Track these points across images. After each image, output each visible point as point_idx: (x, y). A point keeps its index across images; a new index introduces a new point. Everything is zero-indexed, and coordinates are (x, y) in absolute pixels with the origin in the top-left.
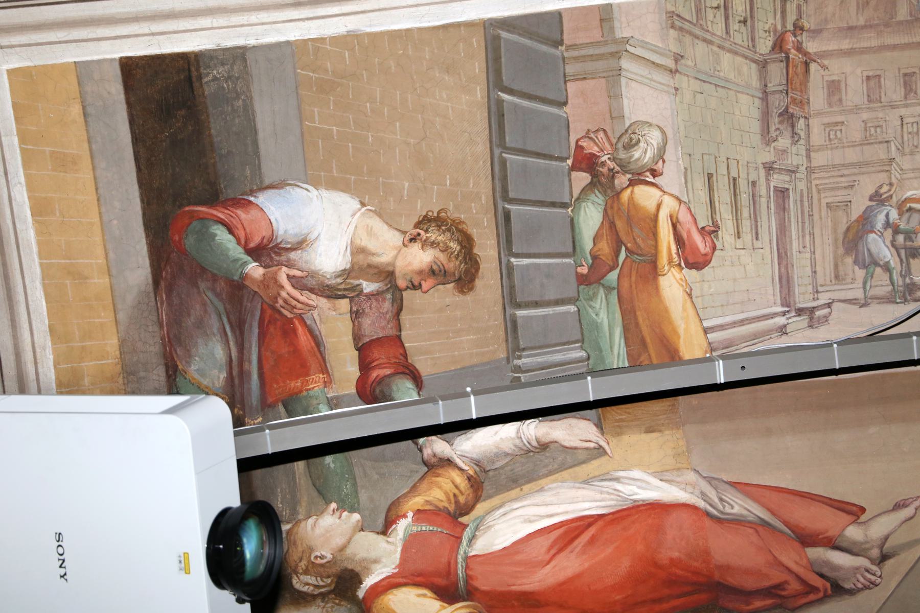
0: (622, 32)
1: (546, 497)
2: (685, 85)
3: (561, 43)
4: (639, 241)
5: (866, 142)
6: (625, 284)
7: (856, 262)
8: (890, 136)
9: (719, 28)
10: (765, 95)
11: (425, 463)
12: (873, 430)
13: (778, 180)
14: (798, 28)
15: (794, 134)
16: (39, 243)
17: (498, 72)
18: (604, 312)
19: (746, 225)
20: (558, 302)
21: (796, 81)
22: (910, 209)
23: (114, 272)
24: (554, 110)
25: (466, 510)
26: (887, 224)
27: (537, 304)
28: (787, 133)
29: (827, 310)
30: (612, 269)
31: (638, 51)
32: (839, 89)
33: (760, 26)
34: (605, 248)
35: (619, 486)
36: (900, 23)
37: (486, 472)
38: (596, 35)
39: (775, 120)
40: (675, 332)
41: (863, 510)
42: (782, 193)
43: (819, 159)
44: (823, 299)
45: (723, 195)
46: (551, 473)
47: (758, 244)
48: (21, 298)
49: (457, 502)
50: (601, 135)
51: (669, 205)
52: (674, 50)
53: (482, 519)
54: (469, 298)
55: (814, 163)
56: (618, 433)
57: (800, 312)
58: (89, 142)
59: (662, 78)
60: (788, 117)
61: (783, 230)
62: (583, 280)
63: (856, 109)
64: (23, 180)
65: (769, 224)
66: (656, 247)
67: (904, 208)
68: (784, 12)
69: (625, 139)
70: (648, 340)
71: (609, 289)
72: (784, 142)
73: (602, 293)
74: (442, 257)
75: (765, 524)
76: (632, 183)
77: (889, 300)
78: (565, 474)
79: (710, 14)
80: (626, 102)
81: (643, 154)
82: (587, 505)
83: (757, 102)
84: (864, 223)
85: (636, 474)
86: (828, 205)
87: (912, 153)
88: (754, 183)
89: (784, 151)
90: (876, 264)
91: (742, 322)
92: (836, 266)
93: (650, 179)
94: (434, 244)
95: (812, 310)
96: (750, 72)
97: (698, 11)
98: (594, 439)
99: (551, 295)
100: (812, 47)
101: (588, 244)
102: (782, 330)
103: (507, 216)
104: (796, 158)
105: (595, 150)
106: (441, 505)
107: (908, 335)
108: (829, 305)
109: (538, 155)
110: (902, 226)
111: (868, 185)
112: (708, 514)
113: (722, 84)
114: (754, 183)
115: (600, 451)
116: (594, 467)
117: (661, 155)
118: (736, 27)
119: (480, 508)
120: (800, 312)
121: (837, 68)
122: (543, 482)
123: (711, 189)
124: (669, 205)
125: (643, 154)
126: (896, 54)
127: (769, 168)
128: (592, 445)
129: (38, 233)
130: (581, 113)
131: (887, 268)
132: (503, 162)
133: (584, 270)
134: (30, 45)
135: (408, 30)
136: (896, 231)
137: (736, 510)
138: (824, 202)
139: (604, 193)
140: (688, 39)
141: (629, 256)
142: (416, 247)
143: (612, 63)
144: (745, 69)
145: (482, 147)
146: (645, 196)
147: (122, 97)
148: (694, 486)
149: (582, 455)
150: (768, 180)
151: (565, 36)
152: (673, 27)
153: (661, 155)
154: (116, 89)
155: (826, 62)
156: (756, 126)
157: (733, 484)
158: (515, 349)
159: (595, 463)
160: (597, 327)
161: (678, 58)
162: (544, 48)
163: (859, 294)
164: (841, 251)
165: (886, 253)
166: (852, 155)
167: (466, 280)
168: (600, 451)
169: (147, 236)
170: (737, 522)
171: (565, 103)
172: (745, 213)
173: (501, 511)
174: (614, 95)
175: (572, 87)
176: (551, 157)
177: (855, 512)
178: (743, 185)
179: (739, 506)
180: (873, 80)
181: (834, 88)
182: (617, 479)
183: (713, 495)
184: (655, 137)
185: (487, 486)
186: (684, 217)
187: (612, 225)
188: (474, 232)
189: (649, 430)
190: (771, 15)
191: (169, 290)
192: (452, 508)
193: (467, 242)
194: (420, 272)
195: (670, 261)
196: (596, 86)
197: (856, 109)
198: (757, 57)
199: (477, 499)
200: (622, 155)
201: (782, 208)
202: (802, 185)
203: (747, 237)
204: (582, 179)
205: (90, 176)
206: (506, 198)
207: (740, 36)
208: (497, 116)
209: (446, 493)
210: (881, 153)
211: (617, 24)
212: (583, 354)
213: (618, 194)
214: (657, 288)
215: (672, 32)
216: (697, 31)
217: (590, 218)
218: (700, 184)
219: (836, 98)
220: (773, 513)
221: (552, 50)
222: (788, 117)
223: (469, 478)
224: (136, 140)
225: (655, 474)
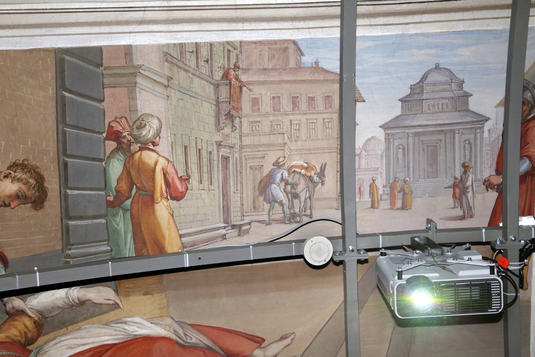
0: (137, 61)
1: (83, 333)
2: (173, 95)
3: (102, 65)
4: (144, 183)
5: (272, 133)
6: (135, 207)
7: (265, 200)
8: (285, 131)
9: (193, 64)
10: (218, 103)
11: (7, 313)
12: (271, 295)
13: (224, 151)
14: (236, 67)
15: (233, 126)
17: (63, 79)
18: (122, 224)
19: (205, 176)
20: (95, 217)
21: (235, 97)
22: (294, 171)
24: (97, 104)
25: (32, 341)
26: (282, 179)
27: (81, 218)
28: (230, 126)
29: (247, 227)
30: (128, 198)
31: (147, 73)
32: (258, 103)
33: (216, 64)
34: (124, 186)
35: (126, 327)
36: (291, 69)
37: (46, 318)
38: (122, 62)
39: (223, 118)
40: (163, 236)
41: (264, 340)
42: (226, 159)
43: (247, 141)
44: (247, 220)
45: (193, 158)
46: (85, 319)
47: (212, 187)
49: (26, 337)
50: (124, 120)
51: (162, 163)
52: (167, 74)
53: (41, 347)
54: (40, 213)
55: (244, 144)
56: (127, 294)
57: (234, 227)
59: (160, 89)
60: (230, 116)
61: (226, 180)
62: (110, 204)
63: (267, 115)
65: (218, 176)
66: (154, 186)
67: (291, 171)
68: (229, 58)
69: (138, 123)
70: (147, 240)
71: (125, 210)
72: (227, 130)
73: (121, 212)
74: (24, 188)
75: (209, 348)
76: (141, 149)
77: (282, 221)
78: (94, 319)
79: (188, 55)
80: (138, 102)
81: (148, 133)
82: (106, 338)
83: (213, 107)
84: (270, 179)
85: (137, 319)
86: (251, 167)
87: (296, 141)
88: (210, 153)
89: (228, 136)
90: (275, 201)
91: (201, 232)
92: (254, 201)
93: (151, 147)
94: (19, 180)
95: (240, 226)
96: (210, 90)
97: (181, 53)
98: (113, 298)
99: (91, 213)
100: (244, 78)
101: (114, 184)
102: (224, 237)
103: (66, 164)
104: (234, 140)
105: (120, 128)
106: (16, 339)
107: (290, 242)
108: (249, 224)
109: (86, 130)
110: (290, 181)
111: (272, 157)
112: (177, 343)
113: (194, 96)
114: (210, 153)
115: (116, 306)
116: (112, 315)
117: (158, 134)
118: (203, 64)
119: (41, 340)
120: (234, 227)
121: (257, 91)
122: (80, 324)
123: (186, 155)
124: (162, 163)
125: (148, 133)
126: (288, 85)
127: (219, 145)
128: (111, 302)
130: (112, 106)
131: (281, 204)
132: (64, 133)
133: (111, 199)
135: (7, 51)
136: (287, 183)
137: (194, 340)
138: (248, 165)
139: (125, 154)
140: (175, 69)
141: (138, 192)
142: (8, 181)
143: (132, 79)
144: (207, 88)
145: (51, 123)
146: (149, 157)
148: (170, 326)
149: (105, 308)
150: (218, 151)
151: (104, 61)
152: (167, 61)
153: (158, 134)
155: (251, 87)
156: (212, 121)
157: (193, 326)
158: (67, 244)
159: (112, 313)
160: (117, 232)
161: (169, 79)
162: (91, 67)
163: (266, 218)
164: (257, 193)
165: (281, 195)
166: (264, 140)
167: (38, 200)
168: (116, 306)
170: (194, 347)
171: (103, 101)
172: (205, 169)
173: (54, 342)
174: (132, 97)
175: (107, 91)
176: (93, 132)
177: (259, 341)
178: (204, 154)
179: (196, 338)
180: (276, 99)
181: (255, 102)
182: (125, 323)
183: (181, 332)
184: (155, 123)
185: (46, 327)
186: (170, 170)
187: (129, 173)
188: (45, 173)
189: (145, 294)
190: (222, 59)
192: (23, 340)
193: (40, 180)
194: (10, 196)
195: (162, 195)
196: (121, 92)
197: (267, 115)
198: (213, 82)
199: (39, 335)
200: (136, 132)
201: (226, 168)
202: (237, 155)
203: (206, 183)
204: (111, 145)
206: (65, 154)
207: (204, 69)
208: (62, 106)
209: (20, 331)
210: (279, 139)
211: (134, 57)
212: (109, 248)
213: (133, 155)
214: (153, 210)
215: (166, 64)
216: (180, 64)
217: (116, 168)
218: (180, 151)
219: (256, 107)
220: (214, 342)
221: (96, 69)
222: (230, 116)
223: (35, 322)
225: (147, 320)
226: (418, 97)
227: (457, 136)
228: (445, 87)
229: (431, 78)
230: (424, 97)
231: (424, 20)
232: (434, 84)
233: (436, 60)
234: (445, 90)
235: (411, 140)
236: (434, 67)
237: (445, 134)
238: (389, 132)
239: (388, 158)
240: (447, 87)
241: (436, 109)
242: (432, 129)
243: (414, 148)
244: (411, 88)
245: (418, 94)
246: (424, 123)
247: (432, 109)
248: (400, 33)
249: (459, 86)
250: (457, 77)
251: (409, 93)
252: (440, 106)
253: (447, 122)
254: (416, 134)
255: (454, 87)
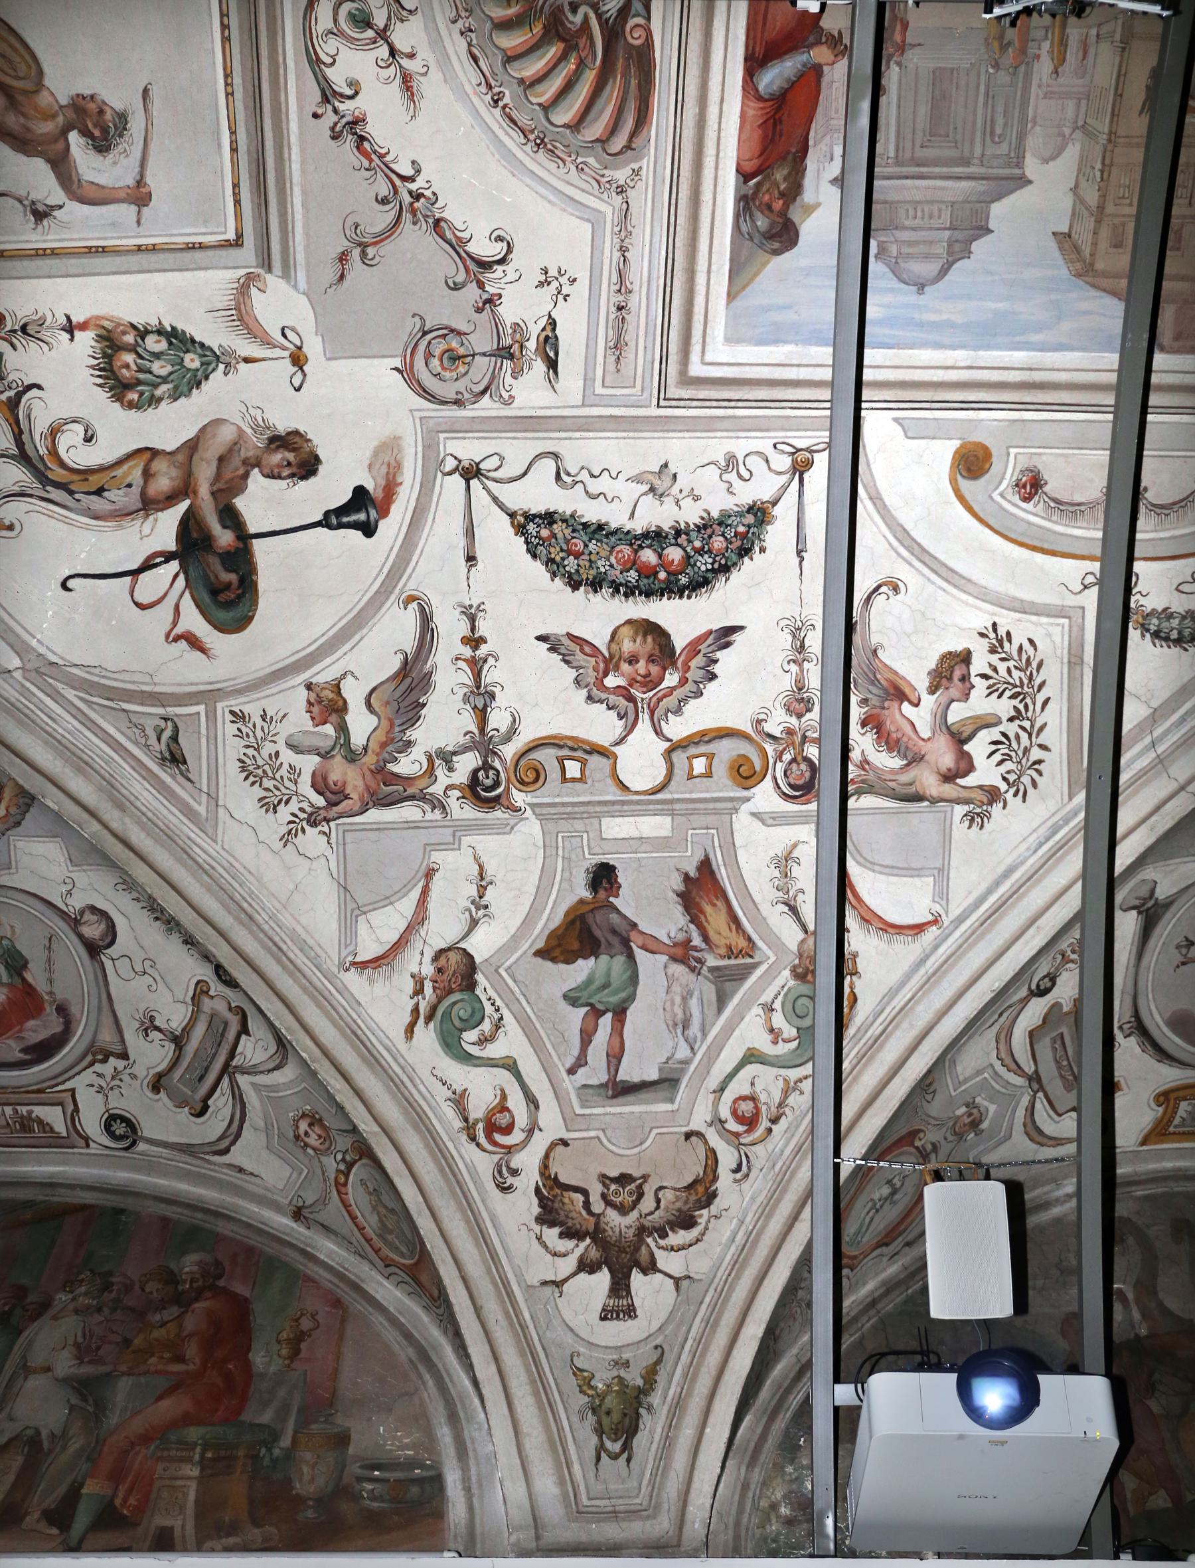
226: (958, 235)
227: (892, 154)
228: (911, 250)
229: (933, 268)
230: (947, 233)
231: (940, 372)
232: (927, 257)
233: (922, 300)
234: (911, 243)
235: (978, 151)
236: (926, 289)
237: (912, 159)
238: (1017, 171)
239: (1023, 120)
240: (906, 250)
241: (926, 210)
242: (937, 170)
243: (973, 133)
244: (970, 252)
245: (957, 241)
246: (949, 183)
247: (935, 208)
248: (981, 353)
249: (884, 249)
250: (888, 266)
251: (974, 245)
252: (919, 214)
253: (908, 182)
254: (966, 162)
255: (894, 249)
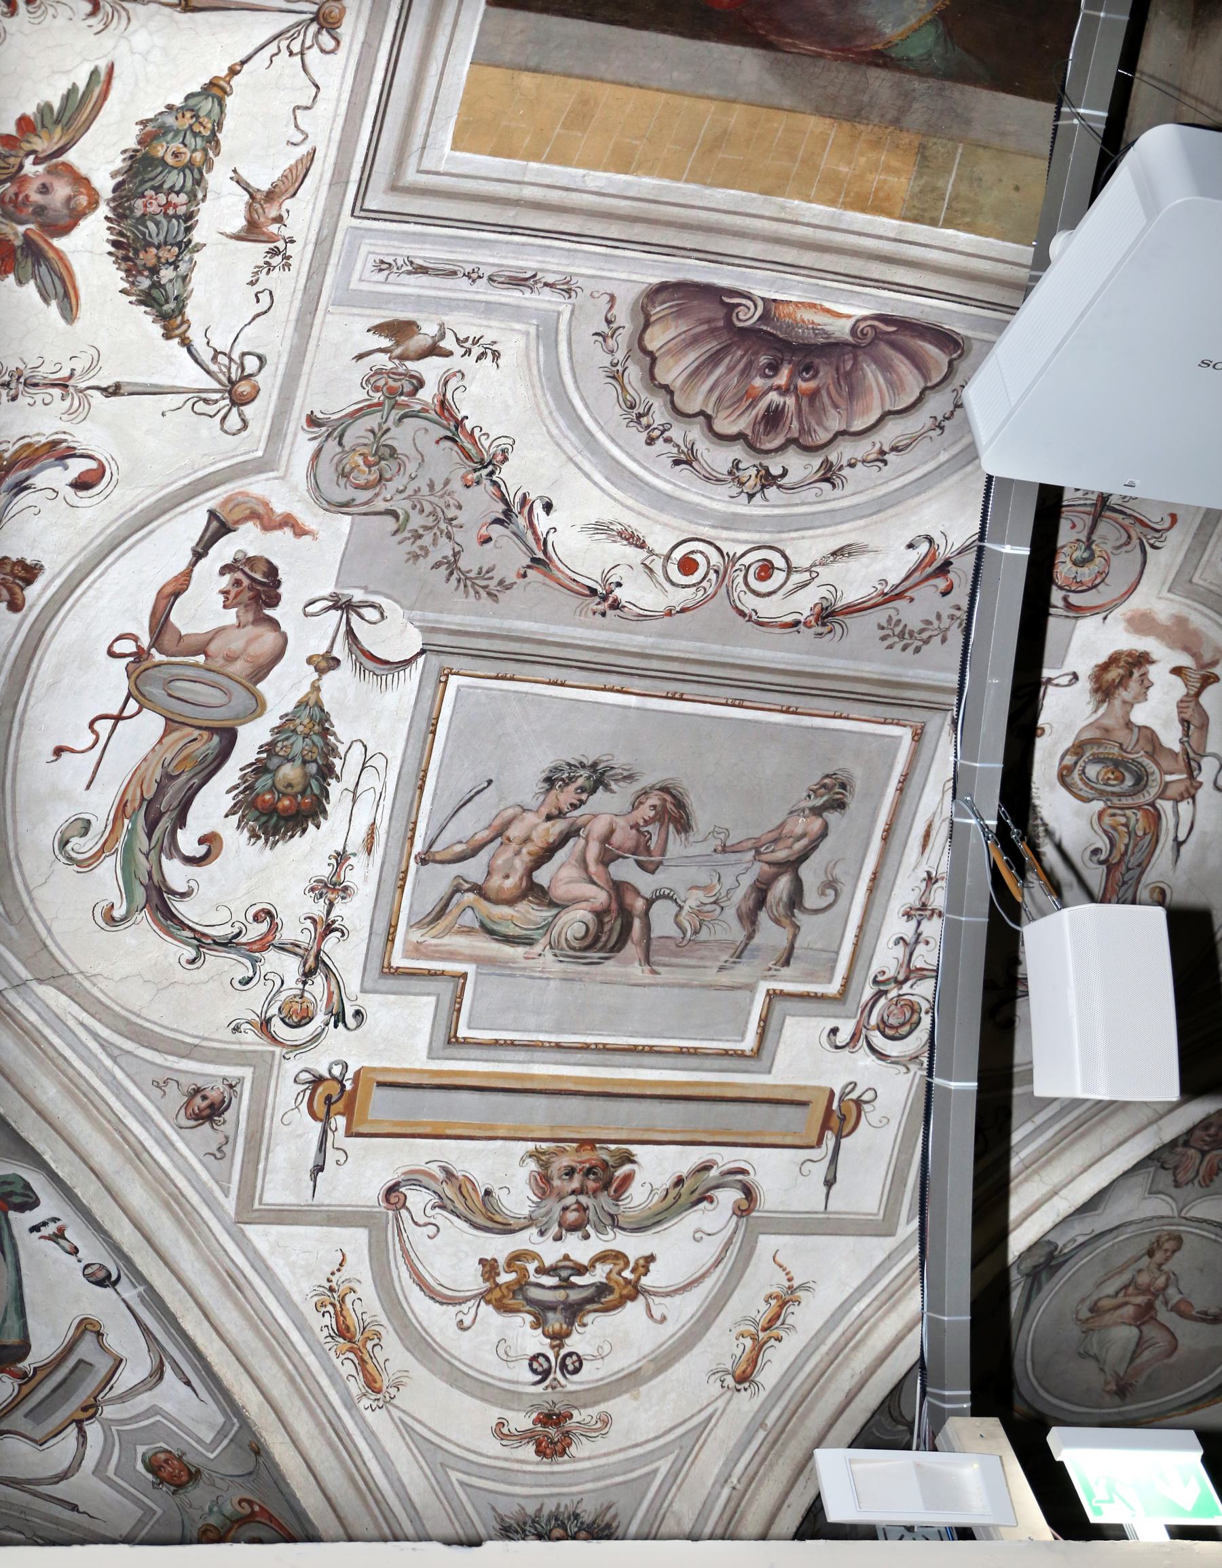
16: (662, 175)
23: (732, 95)
48: (714, 216)
58: (569, 76)
64: (581, 172)
129: (649, 173)
134: (432, 113)
147: (533, 17)
154: (522, 20)
169: (708, 39)
191: (783, 31)
205: (609, 88)
224: (590, 16)
